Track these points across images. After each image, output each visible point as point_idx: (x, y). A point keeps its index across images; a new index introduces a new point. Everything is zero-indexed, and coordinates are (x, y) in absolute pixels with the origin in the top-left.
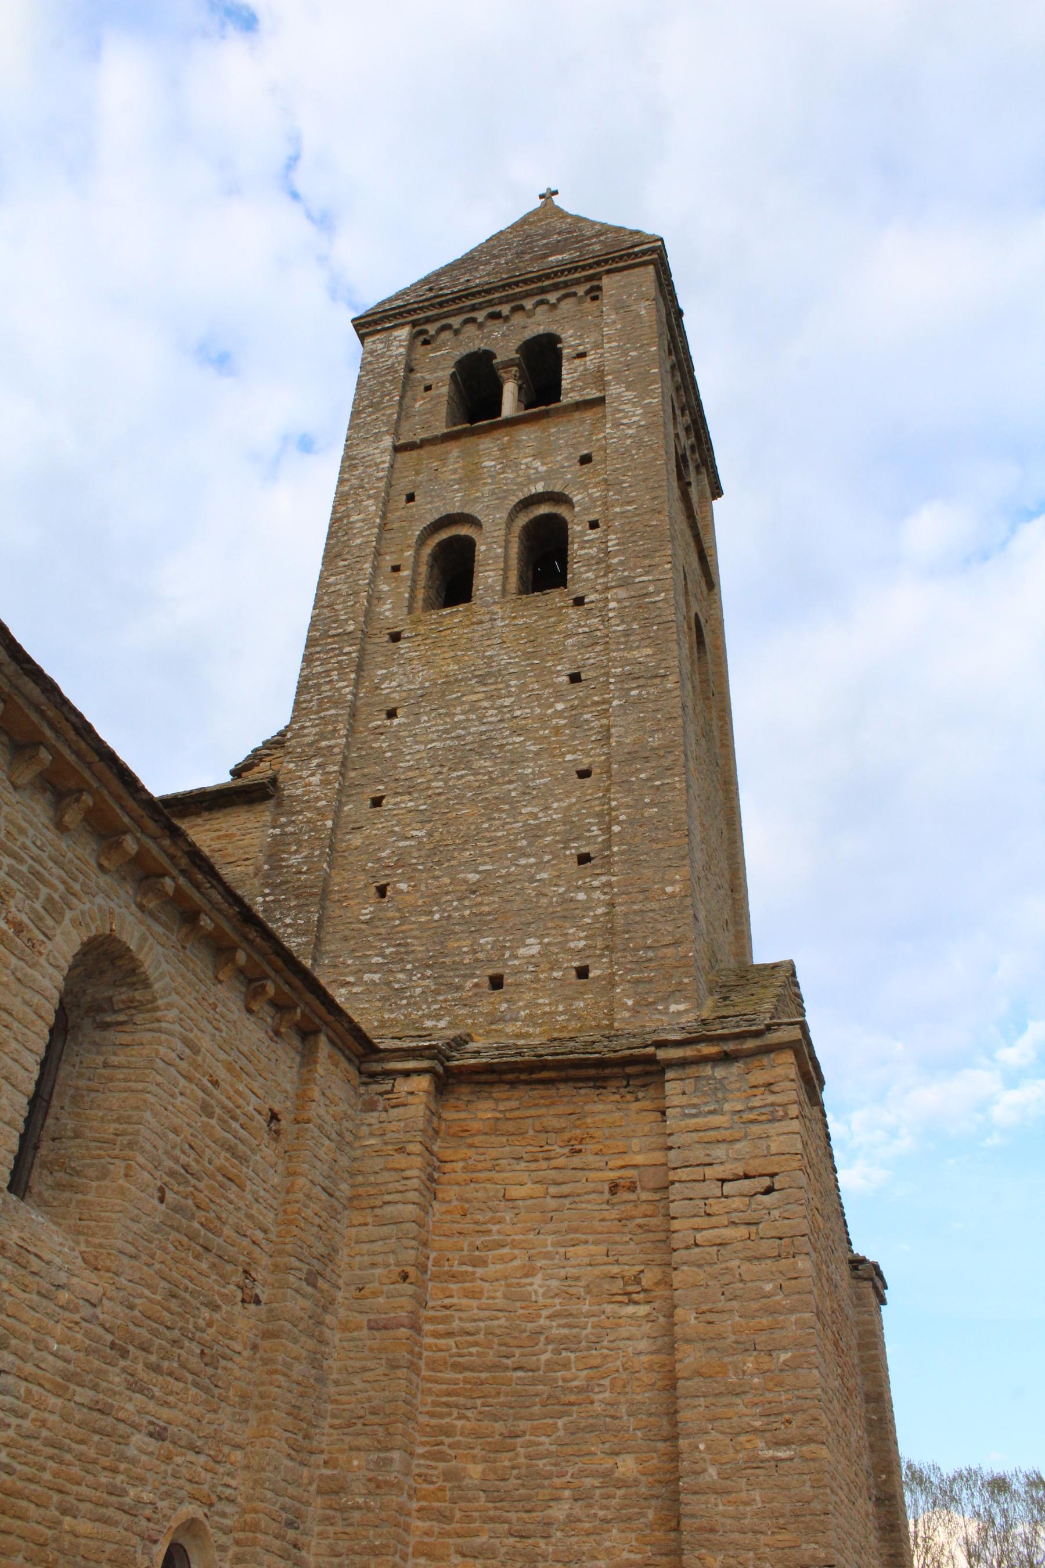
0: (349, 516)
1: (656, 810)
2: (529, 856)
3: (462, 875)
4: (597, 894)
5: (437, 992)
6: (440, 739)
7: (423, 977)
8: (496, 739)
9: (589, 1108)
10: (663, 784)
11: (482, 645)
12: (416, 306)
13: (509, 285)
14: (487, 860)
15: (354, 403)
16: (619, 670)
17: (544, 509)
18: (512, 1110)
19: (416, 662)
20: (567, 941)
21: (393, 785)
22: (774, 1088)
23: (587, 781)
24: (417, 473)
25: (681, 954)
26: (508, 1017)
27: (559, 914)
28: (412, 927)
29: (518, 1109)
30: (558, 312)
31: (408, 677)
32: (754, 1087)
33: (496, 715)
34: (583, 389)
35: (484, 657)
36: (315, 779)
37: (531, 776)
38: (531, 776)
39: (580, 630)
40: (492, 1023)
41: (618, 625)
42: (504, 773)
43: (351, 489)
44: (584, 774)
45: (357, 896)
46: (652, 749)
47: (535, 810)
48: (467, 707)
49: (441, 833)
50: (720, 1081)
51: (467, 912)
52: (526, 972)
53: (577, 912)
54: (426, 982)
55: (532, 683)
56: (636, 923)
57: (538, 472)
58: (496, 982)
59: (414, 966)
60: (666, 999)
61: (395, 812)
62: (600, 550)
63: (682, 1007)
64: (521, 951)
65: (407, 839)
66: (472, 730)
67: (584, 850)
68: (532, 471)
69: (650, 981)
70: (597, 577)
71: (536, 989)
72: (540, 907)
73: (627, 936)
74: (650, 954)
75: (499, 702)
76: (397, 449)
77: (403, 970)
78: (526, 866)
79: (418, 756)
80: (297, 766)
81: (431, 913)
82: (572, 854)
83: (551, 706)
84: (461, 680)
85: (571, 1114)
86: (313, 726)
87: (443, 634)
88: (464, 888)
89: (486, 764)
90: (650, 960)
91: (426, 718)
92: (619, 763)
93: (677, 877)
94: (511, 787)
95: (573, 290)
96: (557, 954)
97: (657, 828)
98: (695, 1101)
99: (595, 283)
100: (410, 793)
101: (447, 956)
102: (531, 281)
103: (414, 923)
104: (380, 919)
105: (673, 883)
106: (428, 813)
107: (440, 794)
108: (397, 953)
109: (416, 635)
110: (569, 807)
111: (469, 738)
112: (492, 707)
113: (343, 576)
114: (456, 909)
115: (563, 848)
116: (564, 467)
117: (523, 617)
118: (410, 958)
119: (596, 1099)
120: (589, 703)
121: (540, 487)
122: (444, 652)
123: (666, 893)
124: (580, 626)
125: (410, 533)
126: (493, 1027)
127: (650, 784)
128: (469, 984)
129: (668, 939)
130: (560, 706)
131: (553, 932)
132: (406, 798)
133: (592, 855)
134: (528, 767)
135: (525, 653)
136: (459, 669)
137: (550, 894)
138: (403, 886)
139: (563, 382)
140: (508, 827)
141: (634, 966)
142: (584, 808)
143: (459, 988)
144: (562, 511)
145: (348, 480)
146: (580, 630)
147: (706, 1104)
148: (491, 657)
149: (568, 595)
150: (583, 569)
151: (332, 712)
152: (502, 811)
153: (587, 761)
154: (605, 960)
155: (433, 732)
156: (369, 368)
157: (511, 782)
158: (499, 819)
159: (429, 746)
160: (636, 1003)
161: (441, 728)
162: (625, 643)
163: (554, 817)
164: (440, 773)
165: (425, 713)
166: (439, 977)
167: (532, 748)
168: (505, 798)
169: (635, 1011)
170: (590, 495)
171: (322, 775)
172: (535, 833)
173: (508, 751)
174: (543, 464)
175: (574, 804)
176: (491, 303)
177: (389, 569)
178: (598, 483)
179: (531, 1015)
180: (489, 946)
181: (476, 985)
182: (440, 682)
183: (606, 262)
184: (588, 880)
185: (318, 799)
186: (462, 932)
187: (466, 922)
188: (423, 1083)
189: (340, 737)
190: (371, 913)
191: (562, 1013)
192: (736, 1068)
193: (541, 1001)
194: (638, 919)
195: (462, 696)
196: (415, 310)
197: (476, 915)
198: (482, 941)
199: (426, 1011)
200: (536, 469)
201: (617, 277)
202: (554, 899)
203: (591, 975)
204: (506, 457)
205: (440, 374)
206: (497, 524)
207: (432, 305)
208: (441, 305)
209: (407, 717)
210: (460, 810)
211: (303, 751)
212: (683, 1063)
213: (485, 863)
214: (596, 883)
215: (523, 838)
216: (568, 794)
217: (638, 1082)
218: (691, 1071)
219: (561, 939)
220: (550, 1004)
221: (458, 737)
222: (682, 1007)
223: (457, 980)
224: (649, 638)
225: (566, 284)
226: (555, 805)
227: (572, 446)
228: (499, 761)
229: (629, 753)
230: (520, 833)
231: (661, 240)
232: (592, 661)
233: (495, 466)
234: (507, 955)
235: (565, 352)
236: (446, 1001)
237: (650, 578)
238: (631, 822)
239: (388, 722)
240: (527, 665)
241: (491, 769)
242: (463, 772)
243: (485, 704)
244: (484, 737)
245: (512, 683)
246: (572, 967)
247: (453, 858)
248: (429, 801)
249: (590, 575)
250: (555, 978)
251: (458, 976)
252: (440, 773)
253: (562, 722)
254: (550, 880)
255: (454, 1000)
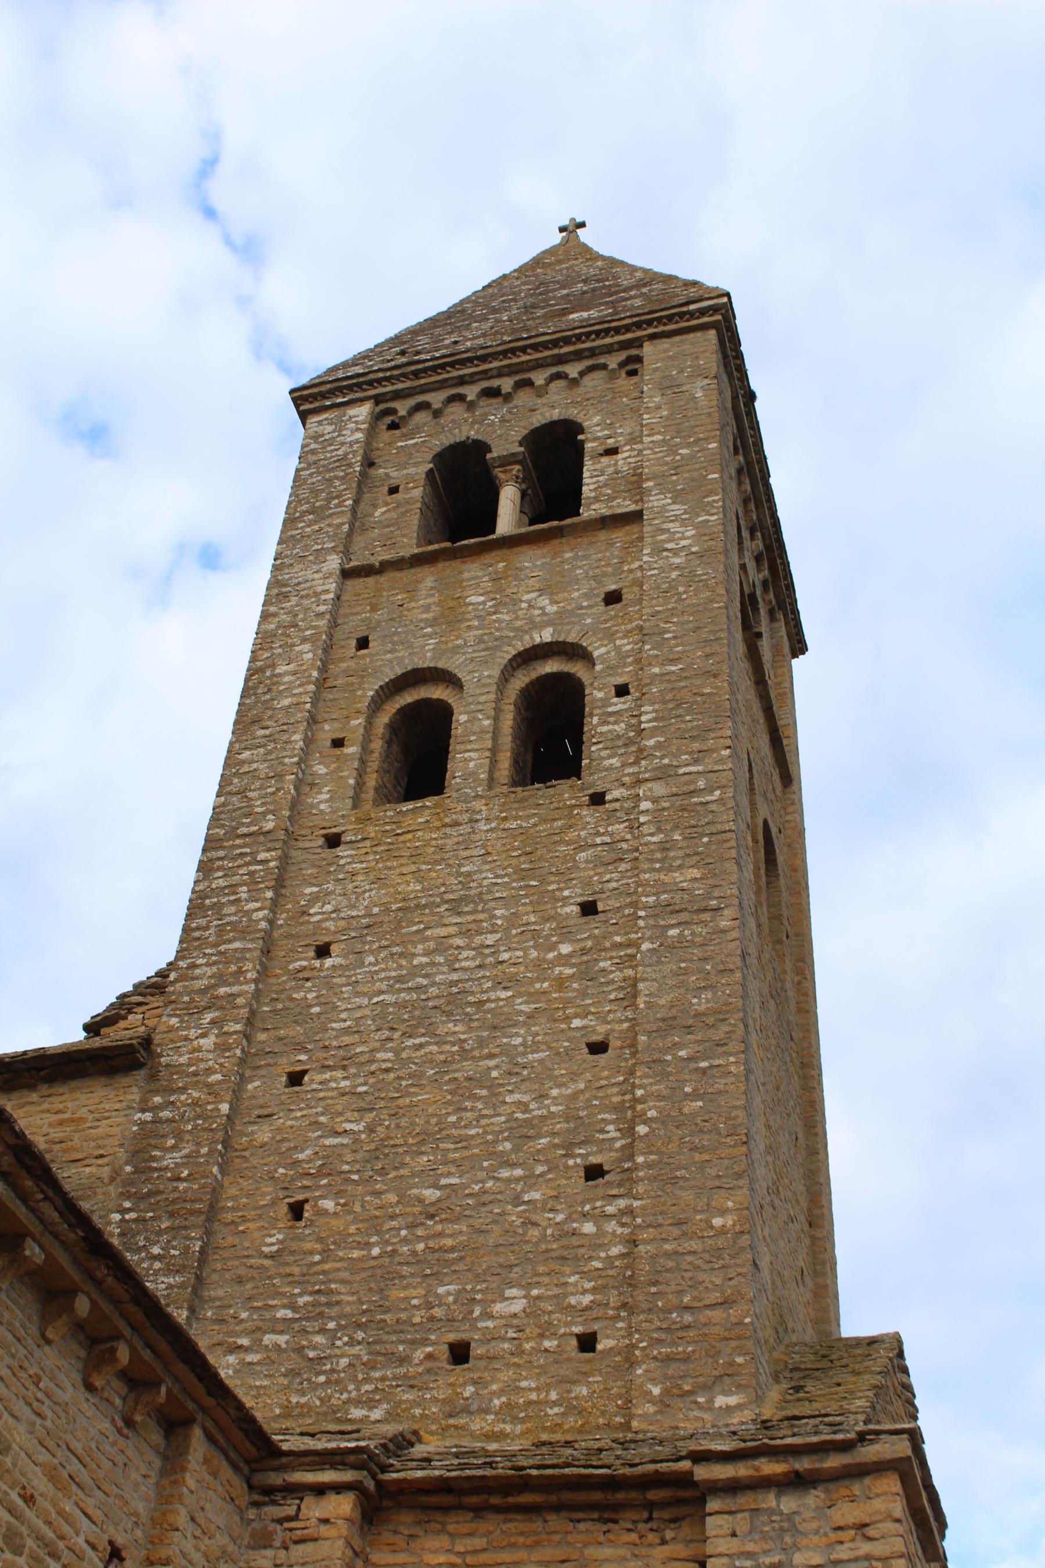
0: (273, 666)
1: (700, 1104)
2: (513, 1165)
3: (415, 1191)
4: (612, 1226)
5: (371, 1366)
6: (390, 990)
7: (352, 1342)
8: (473, 993)
9: (590, 1552)
10: (711, 1067)
11: (456, 857)
12: (381, 375)
13: (513, 351)
14: (453, 1170)
15: (288, 508)
16: (652, 899)
17: (551, 667)
18: (476, 1552)
19: (360, 878)
20: (566, 1295)
21: (321, 1054)
22: (871, 1532)
23: (602, 1059)
24: (374, 609)
25: (734, 1320)
26: (474, 1407)
27: (554, 1254)
28: (339, 1265)
29: (485, 1550)
30: (580, 390)
31: (349, 899)
32: (840, 1528)
33: (473, 959)
34: (612, 499)
35: (459, 874)
36: (208, 1042)
37: (521, 1049)
38: (521, 1049)
39: (598, 840)
40: (451, 1416)
41: (652, 835)
42: (481, 1043)
43: (278, 628)
44: (598, 1048)
45: (260, 1216)
46: (698, 1015)
47: (526, 1098)
48: (432, 945)
49: (388, 1127)
50: (790, 1517)
51: (421, 1247)
52: (504, 1339)
53: (582, 1251)
54: (356, 1350)
55: (527, 914)
56: (668, 1270)
57: (544, 614)
58: (460, 1353)
59: (338, 1324)
60: (707, 1388)
61: (322, 1095)
62: (629, 726)
63: (732, 1400)
64: (498, 1308)
65: (337, 1134)
66: (438, 978)
67: (594, 1160)
68: (537, 612)
69: (687, 1359)
70: (624, 765)
71: (515, 1364)
72: (528, 1242)
73: (653, 1290)
74: (688, 1318)
75: (478, 940)
76: (347, 574)
77: (322, 1331)
78: (509, 1180)
79: (358, 1014)
80: (181, 1022)
81: (368, 1245)
82: (576, 1165)
83: (553, 947)
84: (425, 906)
85: (563, 1561)
86: (207, 965)
87: (401, 838)
88: (417, 1210)
89: (456, 1029)
90: (688, 1327)
91: (372, 959)
92: (649, 1033)
93: (730, 1204)
94: (492, 1063)
95: (602, 360)
96: (551, 1312)
97: (701, 1131)
98: (750, 1547)
99: (634, 352)
100: (344, 1068)
101: (388, 1311)
102: (545, 346)
103: (342, 1259)
104: (293, 1253)
105: (723, 1212)
106: (371, 1098)
107: (387, 1070)
108: (314, 1304)
109: (364, 839)
110: (577, 1094)
111: (434, 991)
112: (468, 947)
113: (262, 750)
114: (404, 1241)
115: (564, 1156)
116: (582, 608)
117: (516, 818)
118: (334, 1312)
119: (602, 1538)
120: (608, 945)
121: (547, 635)
122: (402, 865)
123: (712, 1227)
124: (598, 834)
125: (359, 693)
126: (452, 1421)
127: (692, 1065)
128: (419, 1354)
129: (714, 1297)
130: (565, 949)
131: (546, 1280)
132: (339, 1074)
133: (606, 1168)
134: (517, 1035)
135: (518, 870)
136: (422, 891)
137: (544, 1223)
138: (328, 1204)
139: (584, 488)
140: (484, 1122)
141: (663, 1336)
142: (596, 1098)
143: (404, 1360)
144: (577, 669)
145: (275, 615)
146: (598, 840)
147: (766, 1552)
148: (469, 874)
149: (582, 789)
150: (604, 753)
151: (237, 945)
152: (476, 1098)
153: (602, 1029)
154: (620, 1325)
155: (381, 980)
156: (312, 458)
157: (491, 1056)
158: (473, 1109)
159: (375, 1000)
160: (666, 1392)
161: (393, 974)
162: (662, 861)
163: (553, 1109)
164: (389, 1039)
165: (372, 952)
166: (375, 1342)
167: (523, 1007)
169: (663, 1403)
170: (617, 649)
171: (217, 1036)
173: (489, 1011)
174: (553, 602)
175: (582, 1091)
176: (486, 375)
177: (329, 743)
178: (630, 631)
179: (508, 1405)
180: (451, 1299)
181: (429, 1357)
182: (394, 907)
183: (649, 323)
184: (598, 1204)
185: (209, 1071)
186: (412, 1275)
187: (419, 1262)
188: (344, 1505)
189: (247, 982)
190: (279, 1242)
191: (555, 1403)
192: (814, 1498)
193: (524, 1384)
194: (670, 1264)
195: (426, 928)
196: (379, 381)
197: (433, 1251)
198: (441, 1290)
199: (354, 1394)
200: (542, 608)
201: (664, 344)
202: (549, 1231)
203: (599, 1347)
204: (501, 590)
205: (412, 470)
206: (484, 685)
207: (404, 375)
208: (416, 374)
209: (345, 956)
210: (416, 1094)
211: (192, 1000)
212: (733, 1487)
213: (449, 1174)
214: (610, 1209)
215: (506, 1139)
216: (574, 1076)
217: (666, 1515)
218: (745, 1500)
219: (557, 1291)
220: (537, 1389)
221: (418, 988)
222: (732, 1400)
223: (401, 1348)
224: (697, 854)
225: (593, 353)
226: (555, 1092)
227: (595, 578)
228: (475, 1024)
229: (663, 1020)
230: (502, 1132)
231: (728, 295)
232: (614, 885)
233: (484, 603)
234: (477, 1313)
235: (589, 445)
236: (383, 1379)
237: (700, 768)
238: (663, 1120)
239: (317, 963)
240: (521, 888)
241: (462, 1037)
242: (423, 1040)
243: (458, 941)
244: (455, 990)
245: (498, 913)
246: (571, 1334)
247: (403, 1165)
248: (372, 1081)
249: (615, 761)
250: (546, 1350)
251: (402, 1342)
252: (389, 1039)
253: (569, 971)
254: (544, 1202)
255: (395, 1378)
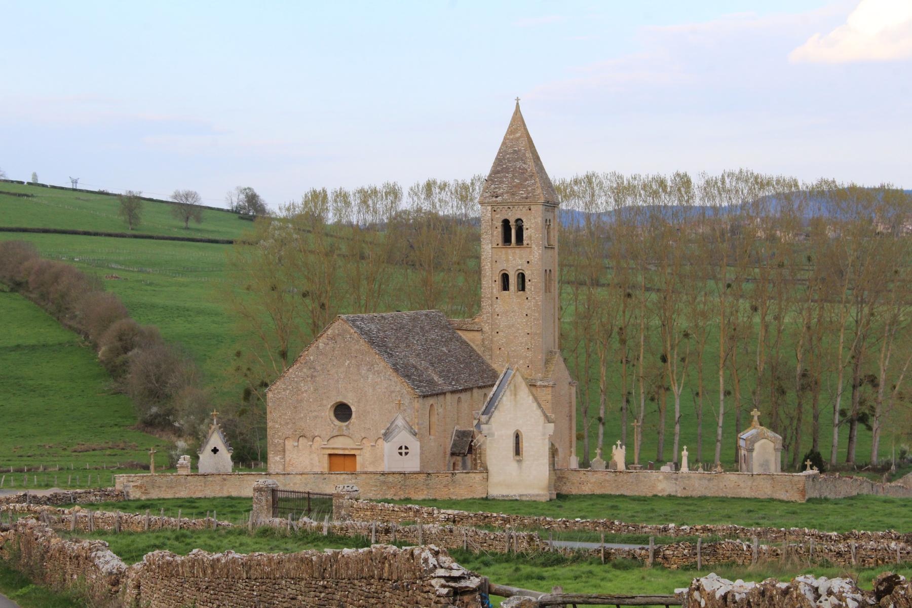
121: (520, 268)
168: (516, 336)
172: (522, 343)
